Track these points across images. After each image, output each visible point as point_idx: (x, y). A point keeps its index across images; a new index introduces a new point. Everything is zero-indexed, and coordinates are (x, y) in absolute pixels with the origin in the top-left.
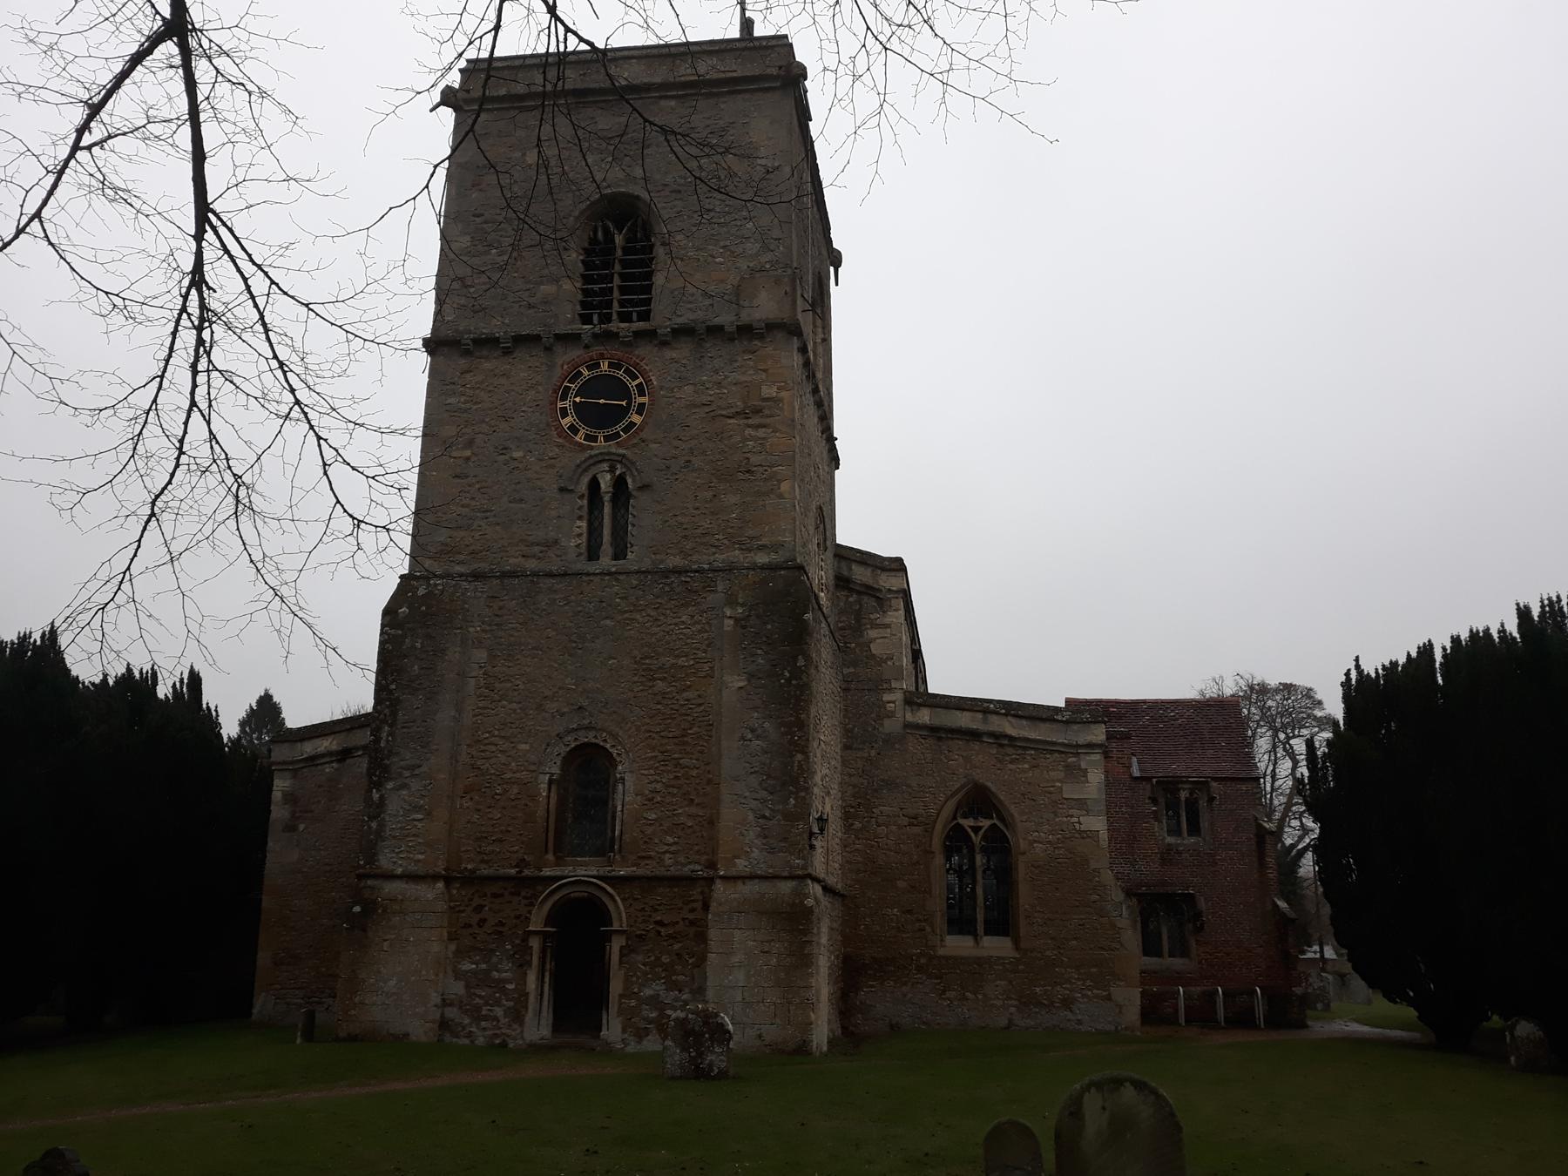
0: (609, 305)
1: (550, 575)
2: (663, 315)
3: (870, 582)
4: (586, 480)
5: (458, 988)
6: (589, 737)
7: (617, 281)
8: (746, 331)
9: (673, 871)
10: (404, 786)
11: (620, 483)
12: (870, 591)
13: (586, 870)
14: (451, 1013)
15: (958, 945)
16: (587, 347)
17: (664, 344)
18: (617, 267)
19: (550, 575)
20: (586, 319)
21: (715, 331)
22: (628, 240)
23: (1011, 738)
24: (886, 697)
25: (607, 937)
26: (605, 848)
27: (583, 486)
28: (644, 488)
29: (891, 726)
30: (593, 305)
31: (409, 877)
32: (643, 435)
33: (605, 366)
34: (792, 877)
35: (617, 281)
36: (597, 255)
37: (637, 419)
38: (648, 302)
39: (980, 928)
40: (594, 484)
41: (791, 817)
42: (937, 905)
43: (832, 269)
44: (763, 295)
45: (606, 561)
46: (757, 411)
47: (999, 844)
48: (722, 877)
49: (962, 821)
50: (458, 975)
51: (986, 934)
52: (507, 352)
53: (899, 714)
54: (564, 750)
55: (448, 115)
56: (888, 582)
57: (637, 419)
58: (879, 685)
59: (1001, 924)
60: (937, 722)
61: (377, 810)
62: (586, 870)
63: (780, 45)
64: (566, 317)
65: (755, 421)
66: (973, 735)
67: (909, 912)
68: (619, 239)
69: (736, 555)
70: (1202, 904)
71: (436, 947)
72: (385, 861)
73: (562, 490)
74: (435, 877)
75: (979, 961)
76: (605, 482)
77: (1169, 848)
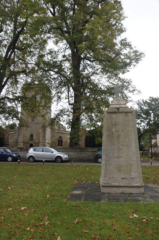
13: (32, 142)
15: (58, 147)
26: (33, 141)
42: (57, 144)
45: (33, 122)
47: (62, 141)
54: (30, 134)
59: (61, 146)
61: (18, 138)
62: (32, 142)
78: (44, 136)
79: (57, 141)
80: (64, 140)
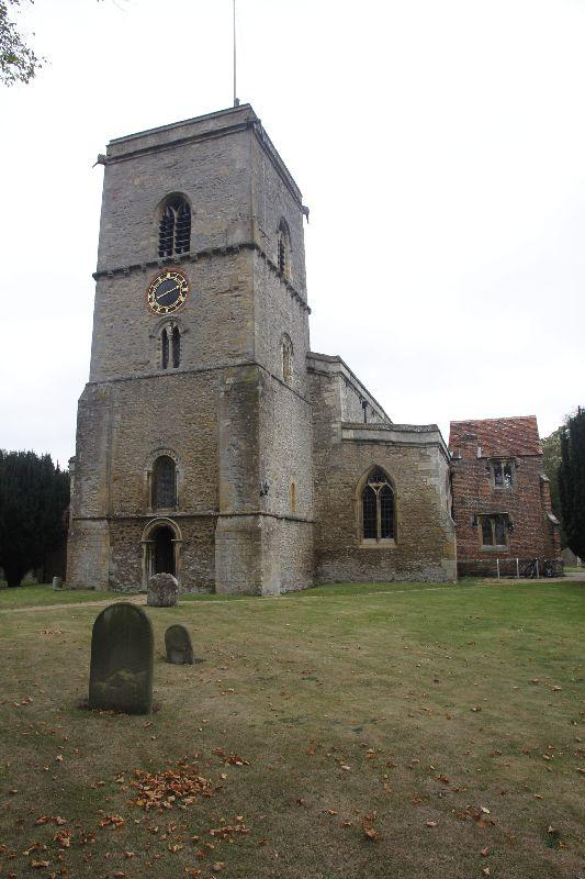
0: (171, 246)
1: (146, 378)
2: (196, 246)
3: (324, 369)
4: (161, 331)
5: (114, 567)
6: (164, 453)
7: (175, 234)
8: (231, 251)
9: (201, 513)
10: (90, 479)
11: (175, 331)
12: (324, 374)
14: (113, 577)
15: (369, 543)
16: (160, 268)
17: (194, 261)
18: (175, 228)
19: (146, 378)
20: (161, 255)
21: (217, 252)
22: (180, 214)
23: (393, 443)
24: (333, 426)
25: (173, 544)
26: (173, 504)
27: (160, 335)
28: (185, 332)
29: (335, 440)
30: (165, 247)
31: (93, 519)
32: (186, 306)
33: (168, 276)
34: (251, 515)
35: (175, 234)
36: (166, 224)
37: (182, 299)
38: (189, 242)
39: (379, 535)
40: (165, 332)
41: (252, 487)
42: (358, 523)
43: (304, 216)
44: (238, 231)
45: (171, 369)
46: (236, 289)
47: (388, 494)
48: (222, 516)
49: (371, 485)
50: (114, 561)
51: (383, 537)
52: (127, 275)
53: (339, 433)
54: (154, 459)
55: (102, 167)
56: (332, 368)
57: (182, 299)
58: (329, 420)
59: (389, 531)
60: (357, 436)
63: (248, 108)
64: (152, 254)
65: (236, 293)
66: (375, 442)
67: (345, 529)
68: (176, 214)
69: (231, 362)
70: (512, 519)
71: (104, 551)
72: (83, 512)
73: (151, 337)
74: (102, 519)
75: (377, 550)
76: (169, 330)
77: (496, 492)
78: (251, 464)
79: (359, 504)
80: (403, 494)
